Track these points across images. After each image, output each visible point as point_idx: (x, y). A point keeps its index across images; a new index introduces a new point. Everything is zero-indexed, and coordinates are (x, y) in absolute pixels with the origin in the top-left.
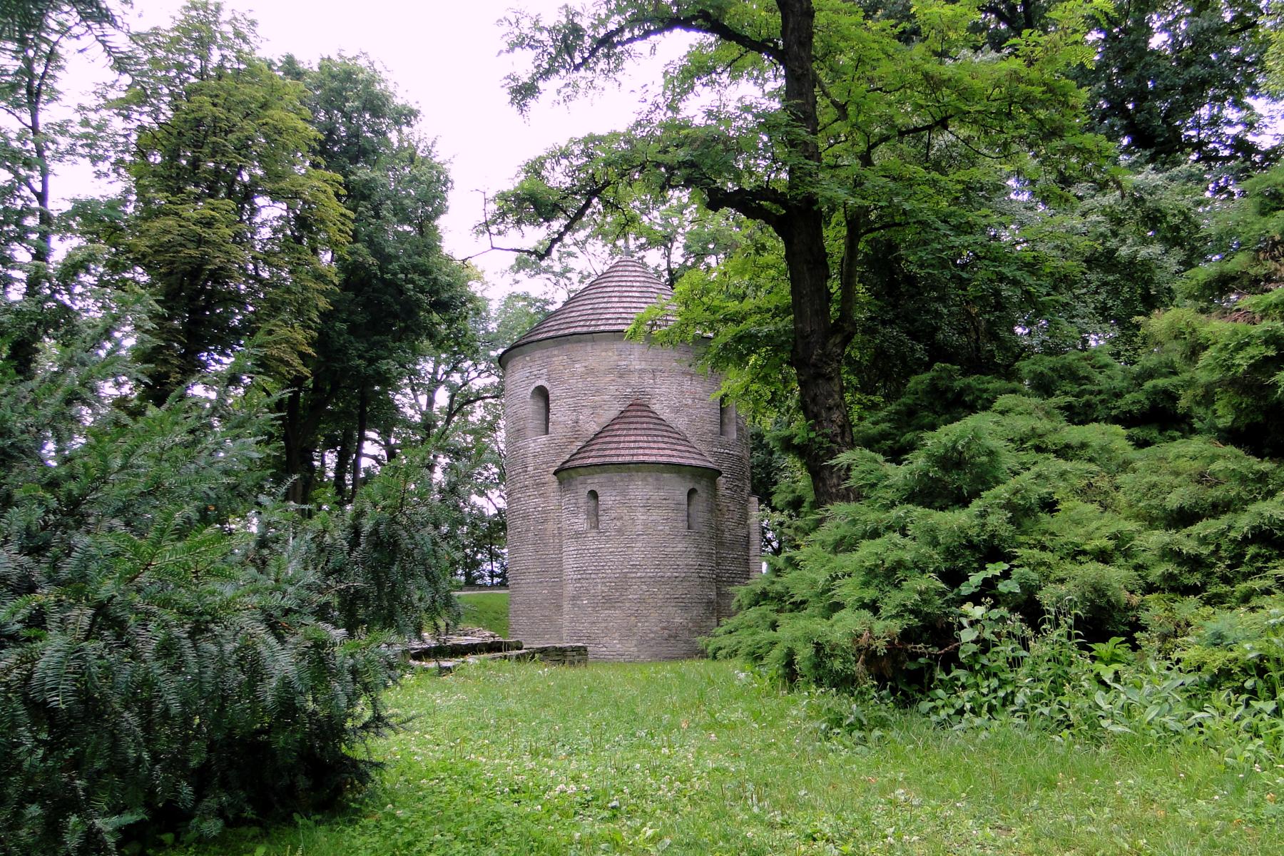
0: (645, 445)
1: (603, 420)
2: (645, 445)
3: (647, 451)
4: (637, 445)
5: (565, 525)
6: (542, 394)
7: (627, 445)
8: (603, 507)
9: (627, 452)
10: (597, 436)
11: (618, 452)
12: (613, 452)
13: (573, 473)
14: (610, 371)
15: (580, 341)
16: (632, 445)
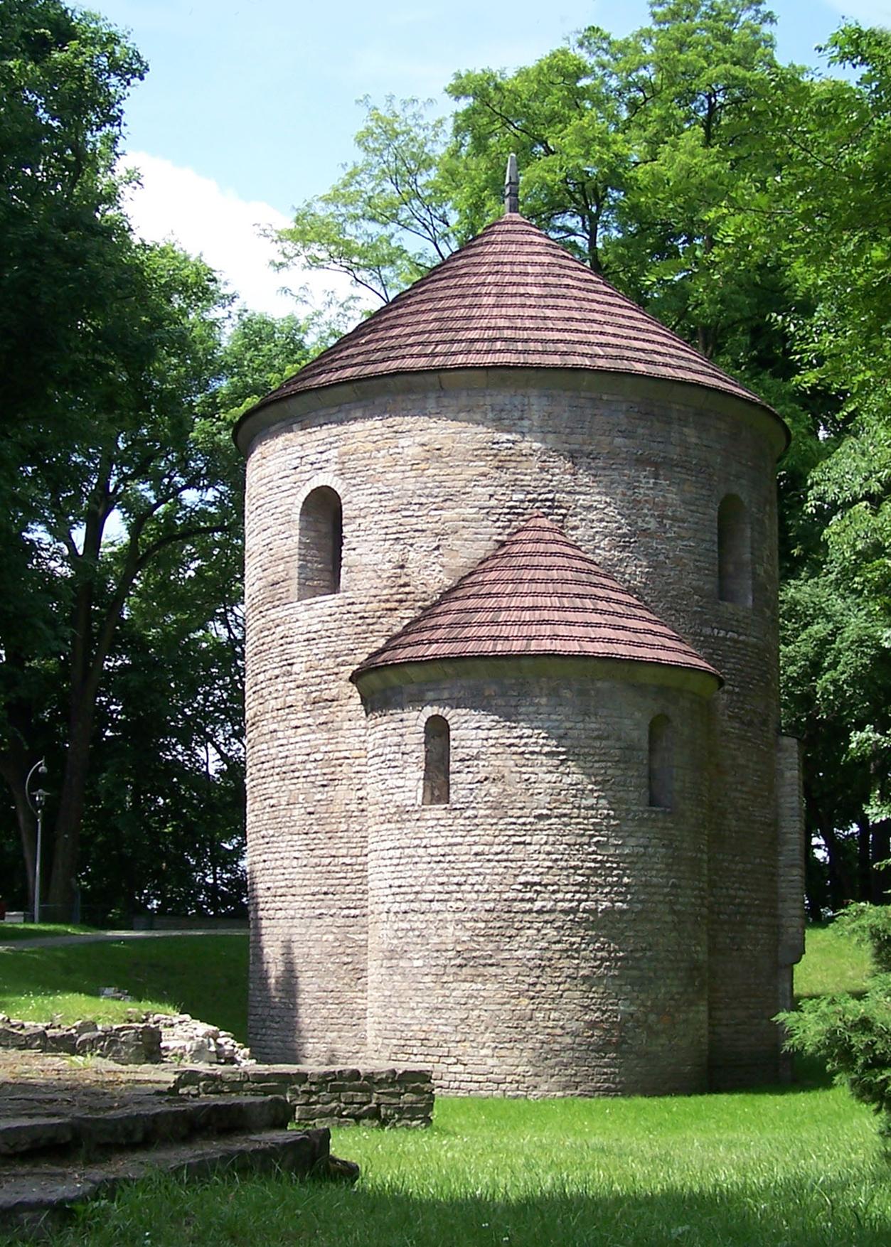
0: (556, 616)
2: (556, 616)
3: (562, 630)
4: (537, 615)
5: (372, 792)
7: (514, 615)
8: (461, 753)
9: (515, 631)
10: (448, 595)
11: (494, 631)
12: (484, 631)
15: (410, 390)
16: (527, 616)
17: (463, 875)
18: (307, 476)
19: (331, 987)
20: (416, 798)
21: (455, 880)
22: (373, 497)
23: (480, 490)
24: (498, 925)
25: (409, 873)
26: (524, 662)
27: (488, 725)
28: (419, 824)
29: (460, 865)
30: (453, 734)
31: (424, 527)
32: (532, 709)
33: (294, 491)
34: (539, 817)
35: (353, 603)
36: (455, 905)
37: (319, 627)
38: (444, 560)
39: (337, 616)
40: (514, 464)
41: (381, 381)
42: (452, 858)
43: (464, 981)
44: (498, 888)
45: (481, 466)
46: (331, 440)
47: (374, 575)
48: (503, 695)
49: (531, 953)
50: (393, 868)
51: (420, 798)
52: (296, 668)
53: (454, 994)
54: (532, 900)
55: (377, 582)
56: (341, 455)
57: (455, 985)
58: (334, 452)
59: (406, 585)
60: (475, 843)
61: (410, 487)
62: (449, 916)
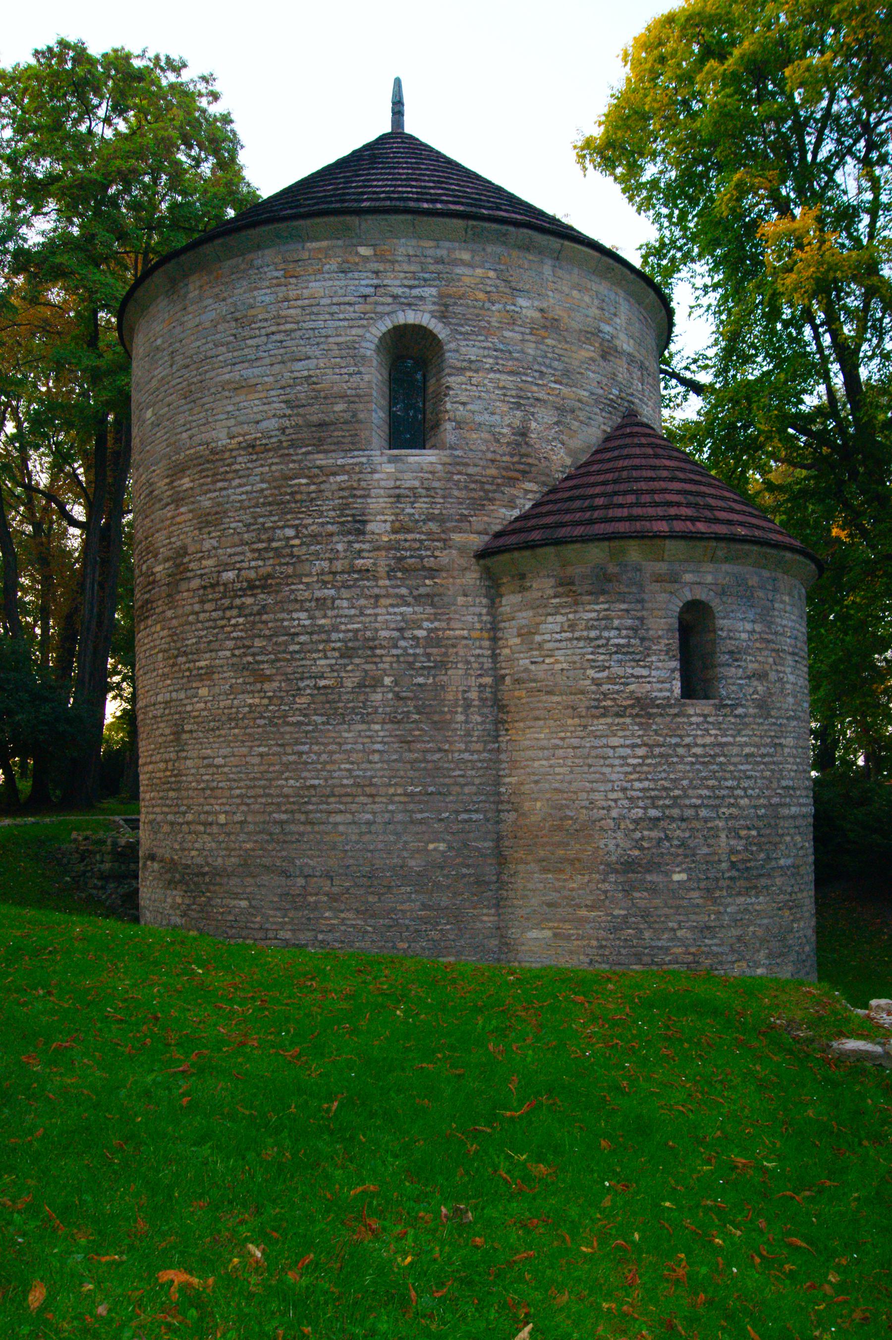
8: (730, 645)
13: (634, 553)
15: (527, 248)
17: (734, 778)
18: (388, 309)
20: (672, 692)
21: (729, 783)
22: (486, 353)
23: (591, 375)
24: (768, 832)
25: (663, 775)
26: (788, 555)
28: (679, 720)
29: (732, 768)
30: (721, 623)
31: (546, 397)
32: (782, 606)
33: (365, 322)
34: (788, 718)
35: (466, 465)
36: (727, 812)
37: (417, 483)
38: (565, 438)
40: (613, 359)
41: (504, 228)
42: (722, 759)
43: (739, 894)
44: (767, 793)
45: (587, 352)
46: (426, 276)
47: (491, 438)
48: (763, 587)
49: (789, 861)
50: (629, 769)
51: (677, 691)
52: (370, 527)
53: (729, 910)
54: (789, 805)
55: (494, 447)
56: (441, 296)
57: (729, 900)
58: (434, 291)
59: (527, 455)
60: (746, 744)
61: (530, 351)
62: (721, 824)
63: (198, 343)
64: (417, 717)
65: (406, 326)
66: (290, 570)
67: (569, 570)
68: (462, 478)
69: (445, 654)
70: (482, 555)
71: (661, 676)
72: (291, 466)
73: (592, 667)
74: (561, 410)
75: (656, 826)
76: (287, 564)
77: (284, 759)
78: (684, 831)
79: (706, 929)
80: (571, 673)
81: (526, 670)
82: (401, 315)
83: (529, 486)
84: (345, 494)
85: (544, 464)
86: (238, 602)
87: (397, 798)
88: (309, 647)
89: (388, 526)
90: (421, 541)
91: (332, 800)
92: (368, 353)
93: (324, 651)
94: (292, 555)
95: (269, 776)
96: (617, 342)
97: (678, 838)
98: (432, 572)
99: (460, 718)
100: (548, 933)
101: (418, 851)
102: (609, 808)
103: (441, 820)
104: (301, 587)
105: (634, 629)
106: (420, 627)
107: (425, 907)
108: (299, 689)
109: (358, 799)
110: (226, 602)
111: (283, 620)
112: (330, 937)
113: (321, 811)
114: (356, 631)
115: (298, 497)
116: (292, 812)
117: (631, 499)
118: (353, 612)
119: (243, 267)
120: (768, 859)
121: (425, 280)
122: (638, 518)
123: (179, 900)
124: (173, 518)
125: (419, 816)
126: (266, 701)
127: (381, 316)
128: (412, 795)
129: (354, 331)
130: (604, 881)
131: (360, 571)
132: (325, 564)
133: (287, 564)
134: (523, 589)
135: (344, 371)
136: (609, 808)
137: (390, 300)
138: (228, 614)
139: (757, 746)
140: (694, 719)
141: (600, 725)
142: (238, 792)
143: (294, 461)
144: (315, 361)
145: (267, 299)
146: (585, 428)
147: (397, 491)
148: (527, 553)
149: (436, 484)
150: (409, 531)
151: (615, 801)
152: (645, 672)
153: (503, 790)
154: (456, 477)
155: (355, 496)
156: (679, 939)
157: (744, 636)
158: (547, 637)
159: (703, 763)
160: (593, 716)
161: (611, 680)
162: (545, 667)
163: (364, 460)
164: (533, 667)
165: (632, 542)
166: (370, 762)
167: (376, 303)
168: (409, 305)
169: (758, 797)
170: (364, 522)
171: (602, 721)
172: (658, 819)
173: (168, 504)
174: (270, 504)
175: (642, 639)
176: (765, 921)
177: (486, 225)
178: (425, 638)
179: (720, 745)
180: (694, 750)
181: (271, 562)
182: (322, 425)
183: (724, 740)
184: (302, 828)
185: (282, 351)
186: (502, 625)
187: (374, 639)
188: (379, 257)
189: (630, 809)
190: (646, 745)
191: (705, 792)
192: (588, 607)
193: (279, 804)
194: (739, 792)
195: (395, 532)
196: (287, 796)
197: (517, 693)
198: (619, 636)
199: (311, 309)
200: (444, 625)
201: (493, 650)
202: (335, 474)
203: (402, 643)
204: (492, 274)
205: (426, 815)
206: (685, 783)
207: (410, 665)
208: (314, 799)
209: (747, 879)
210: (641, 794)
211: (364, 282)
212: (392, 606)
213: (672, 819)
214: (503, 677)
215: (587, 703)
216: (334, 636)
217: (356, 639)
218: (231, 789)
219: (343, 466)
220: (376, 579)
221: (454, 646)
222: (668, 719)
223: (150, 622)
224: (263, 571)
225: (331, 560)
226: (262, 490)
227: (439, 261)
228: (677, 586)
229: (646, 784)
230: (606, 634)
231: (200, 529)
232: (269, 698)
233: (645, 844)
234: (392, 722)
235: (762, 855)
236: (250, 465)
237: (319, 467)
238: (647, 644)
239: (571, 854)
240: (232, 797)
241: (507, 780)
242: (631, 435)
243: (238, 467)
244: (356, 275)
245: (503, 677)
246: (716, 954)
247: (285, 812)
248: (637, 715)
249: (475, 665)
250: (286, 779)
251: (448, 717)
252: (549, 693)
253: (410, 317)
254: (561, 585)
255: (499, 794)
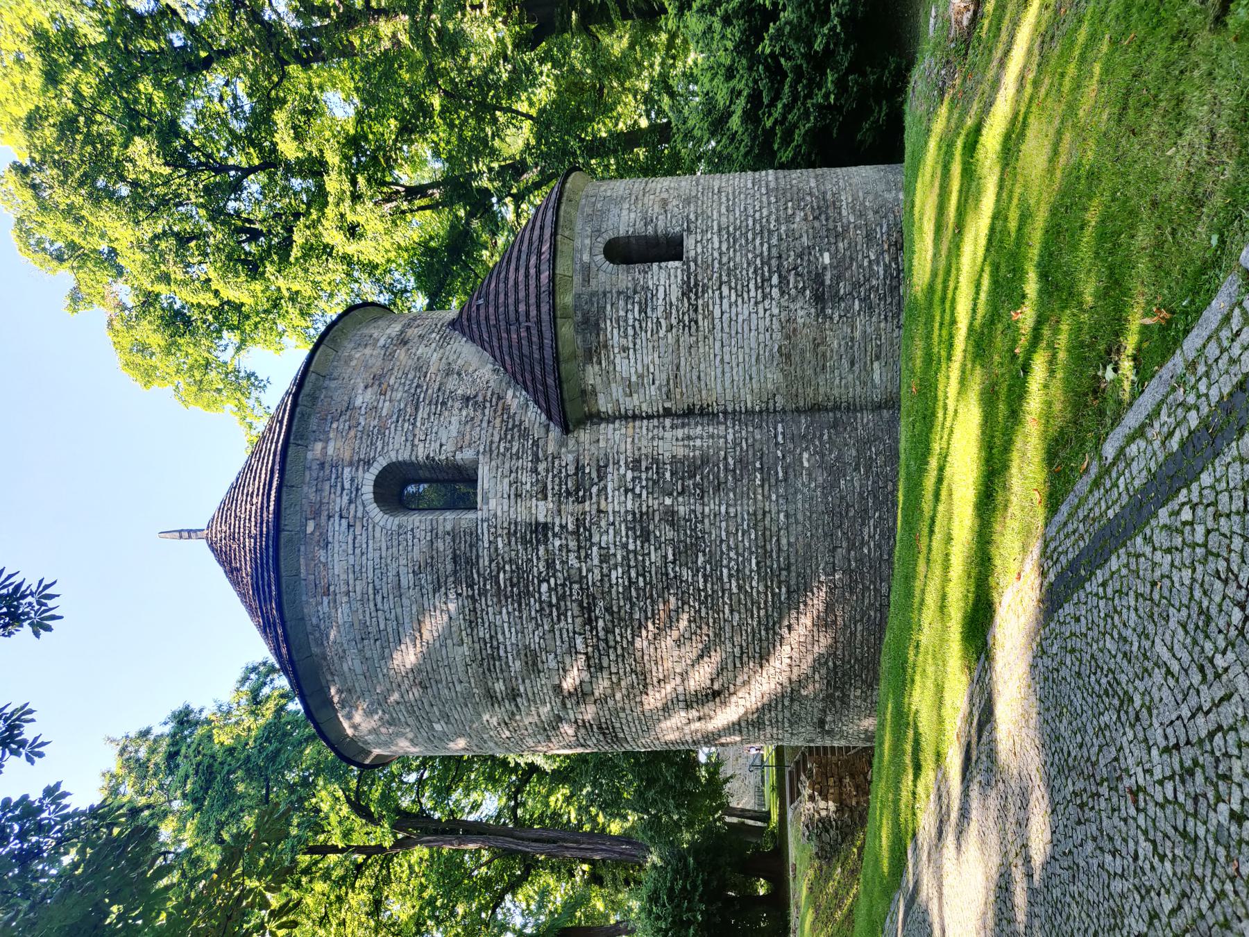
1: (475, 362)
6: (396, 488)
8: (640, 225)
13: (566, 299)
14: (389, 356)
15: (314, 398)
18: (360, 508)
19: (854, 453)
21: (750, 222)
25: (744, 272)
26: (568, 185)
27: (618, 211)
30: (622, 233)
35: (492, 442)
36: (773, 223)
37: (506, 481)
39: (499, 462)
41: (297, 415)
42: (731, 229)
43: (840, 213)
44: (758, 195)
50: (740, 300)
51: (677, 264)
52: (541, 519)
55: (477, 421)
56: (351, 464)
58: (347, 470)
60: (719, 212)
61: (399, 395)
62: (783, 228)
63: (380, 676)
64: (698, 477)
65: (374, 493)
66: (576, 586)
67: (580, 352)
68: (502, 445)
69: (647, 456)
70: (566, 430)
71: (664, 279)
72: (488, 587)
73: (657, 332)
74: (448, 373)
75: (786, 277)
76: (571, 589)
77: (735, 590)
78: (789, 256)
79: (869, 237)
80: (662, 350)
81: (660, 388)
82: (364, 497)
83: (510, 393)
84: (513, 539)
85: (492, 384)
86: (602, 634)
87: (766, 493)
88: (640, 568)
89: (541, 503)
90: (554, 477)
91: (768, 547)
92: (396, 522)
93: (643, 555)
94: (564, 585)
95: (749, 604)
96: (394, 334)
97: (795, 260)
98: (579, 468)
99: (698, 443)
100: (876, 365)
101: (810, 474)
102: (772, 316)
103: (784, 456)
104: (590, 575)
105: (628, 297)
106: (625, 475)
107: (857, 469)
108: (675, 577)
109: (768, 525)
110: (602, 645)
111: (618, 593)
112: (885, 548)
113: (778, 557)
114: (627, 529)
115: (515, 580)
116: (780, 583)
117: (522, 308)
118: (611, 531)
119: (317, 635)
120: (810, 194)
121: (337, 478)
122: (538, 297)
123: (858, 692)
124: (529, 700)
125: (781, 474)
126: (686, 608)
127: (365, 512)
128: (763, 480)
129: (377, 534)
130: (831, 318)
131: (578, 527)
132: (572, 556)
133: (571, 589)
134: (594, 392)
135: (410, 543)
136: (772, 316)
137: (353, 506)
138: (612, 643)
139: (721, 204)
140: (699, 250)
141: (704, 324)
142: (763, 633)
143: (485, 585)
144: (401, 568)
145: (346, 610)
146: (463, 355)
147: (512, 496)
148: (565, 386)
149: (507, 466)
150: (545, 487)
151: (765, 310)
152: (661, 289)
153: (757, 408)
154: (502, 450)
155: (515, 532)
156: (877, 258)
157: (633, 215)
158: (633, 370)
159: (734, 242)
160: (697, 331)
161: (668, 317)
162: (657, 373)
163: (485, 525)
164: (657, 383)
165: (558, 300)
166: (736, 515)
167: (355, 517)
168: (357, 490)
169: (761, 202)
170: (537, 524)
171: (700, 323)
172: (780, 276)
173: (517, 706)
174: (520, 605)
175: (635, 292)
176: (861, 194)
177: (294, 428)
178: (632, 470)
179: (720, 230)
180: (724, 249)
181: (569, 603)
182: (455, 559)
183: (716, 228)
184: (793, 574)
185: (391, 597)
186: (623, 411)
187: (634, 514)
188: (316, 515)
189: (772, 299)
190: (720, 288)
191: (758, 242)
192: (609, 336)
193: (773, 595)
194: (757, 215)
195: (545, 498)
196: (766, 587)
197: (678, 397)
198: (633, 311)
199: (356, 571)
200: (622, 457)
201: (642, 418)
202: (496, 549)
203: (637, 490)
204: (335, 425)
205: (779, 469)
206: (750, 256)
207: (655, 483)
208: (768, 563)
209: (827, 207)
210: (760, 291)
211: (337, 528)
212: (606, 499)
213: (779, 266)
214: (664, 409)
215: (687, 335)
216: (631, 547)
217: (634, 529)
218: (760, 640)
219: (490, 542)
220: (584, 513)
221: (640, 449)
222: (699, 270)
223: (618, 725)
224: (576, 613)
225: (568, 551)
226: (508, 613)
227: (322, 465)
228: (593, 265)
229: (752, 286)
230: (631, 322)
231: (539, 672)
232: (683, 604)
233: (801, 285)
234: (702, 498)
235: (808, 198)
236: (487, 625)
237: (491, 561)
238: (639, 289)
239: (809, 346)
240: (768, 639)
241: (749, 405)
242: (469, 320)
243: (488, 636)
244: (330, 534)
245: (664, 409)
246: (889, 228)
247: (780, 588)
248: (696, 294)
249: (655, 432)
250: (752, 588)
251: (697, 453)
252: (678, 368)
253: (368, 490)
254: (591, 359)
255: (761, 412)
